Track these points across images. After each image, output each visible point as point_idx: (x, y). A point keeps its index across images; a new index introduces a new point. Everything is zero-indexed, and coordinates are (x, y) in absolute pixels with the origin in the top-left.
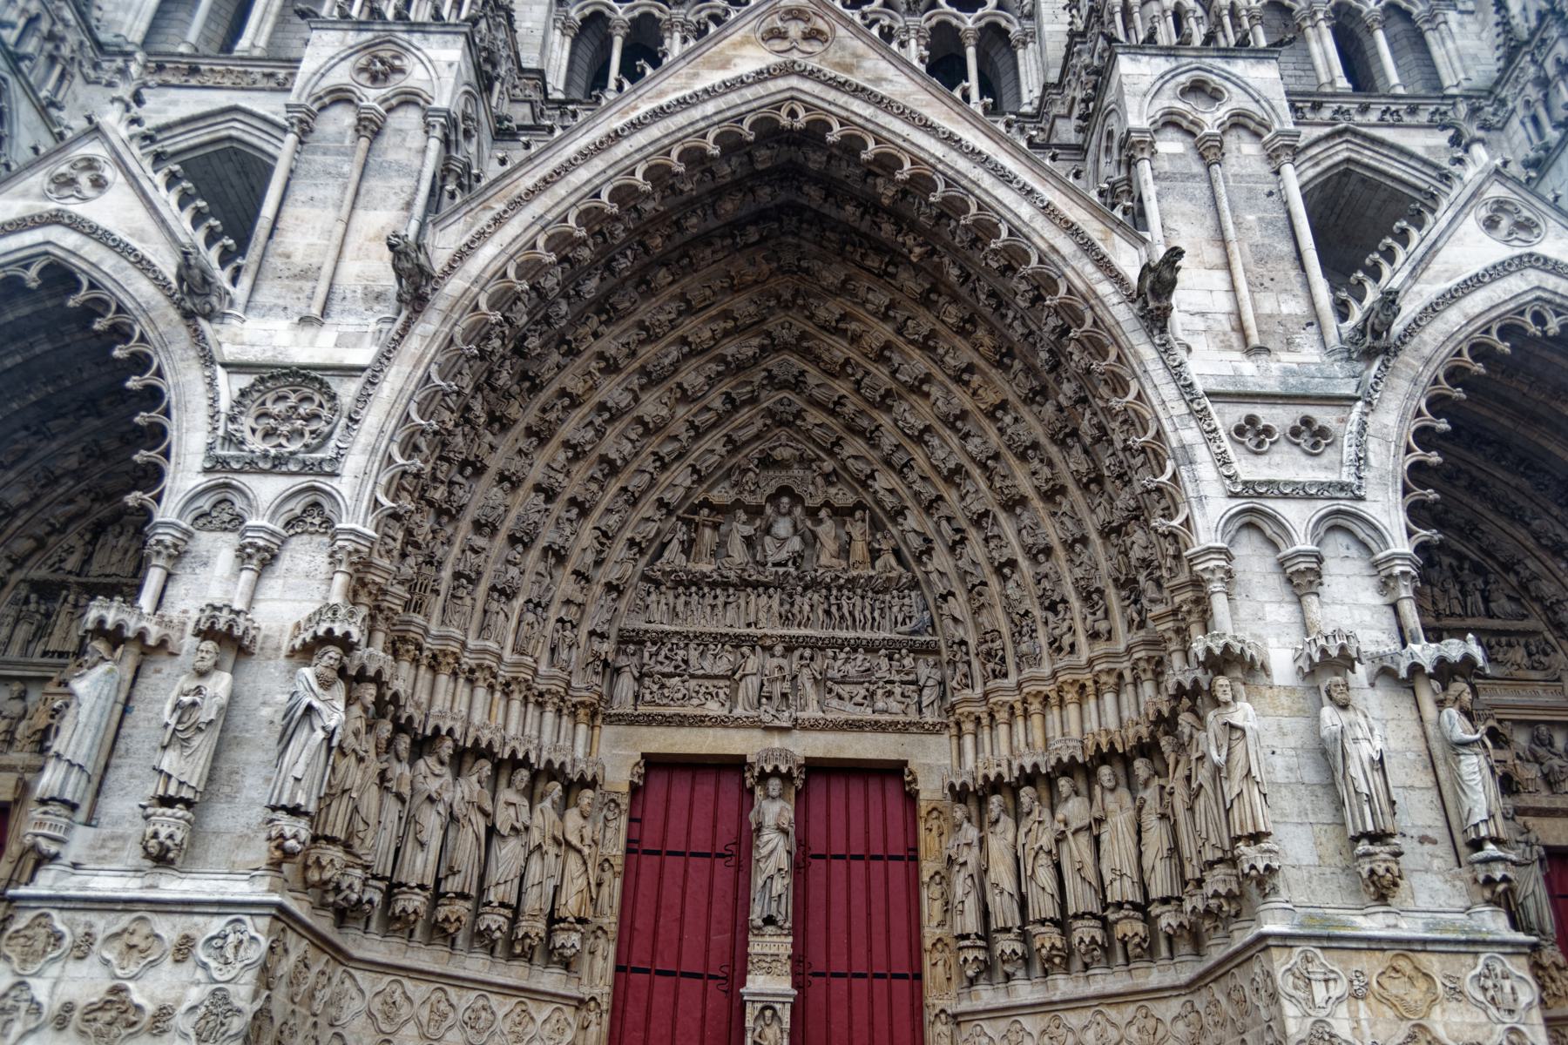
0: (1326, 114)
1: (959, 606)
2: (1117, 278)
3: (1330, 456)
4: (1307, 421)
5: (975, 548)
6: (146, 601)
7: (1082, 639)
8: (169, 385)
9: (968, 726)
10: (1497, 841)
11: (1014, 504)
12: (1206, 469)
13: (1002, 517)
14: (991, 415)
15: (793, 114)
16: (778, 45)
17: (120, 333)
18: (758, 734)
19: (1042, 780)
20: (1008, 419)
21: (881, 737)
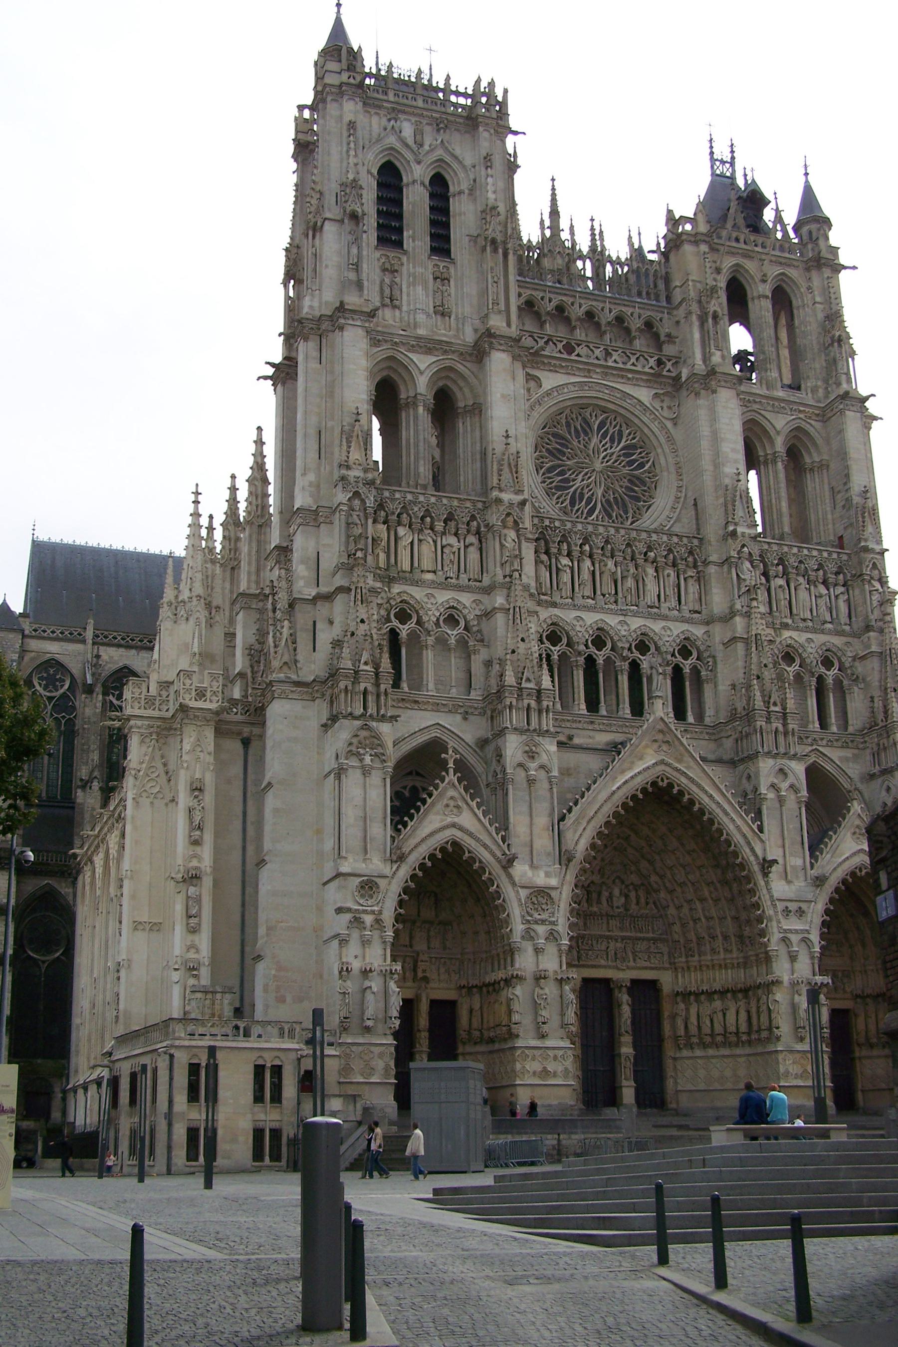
0: (810, 740)
1: (677, 928)
2: (756, 856)
3: (804, 919)
4: (800, 908)
5: (685, 910)
7: (722, 950)
9: (680, 970)
11: (702, 900)
12: (774, 924)
13: (697, 902)
14: (699, 868)
15: (662, 780)
16: (656, 745)
18: (616, 971)
19: (710, 995)
20: (704, 871)
21: (653, 972)
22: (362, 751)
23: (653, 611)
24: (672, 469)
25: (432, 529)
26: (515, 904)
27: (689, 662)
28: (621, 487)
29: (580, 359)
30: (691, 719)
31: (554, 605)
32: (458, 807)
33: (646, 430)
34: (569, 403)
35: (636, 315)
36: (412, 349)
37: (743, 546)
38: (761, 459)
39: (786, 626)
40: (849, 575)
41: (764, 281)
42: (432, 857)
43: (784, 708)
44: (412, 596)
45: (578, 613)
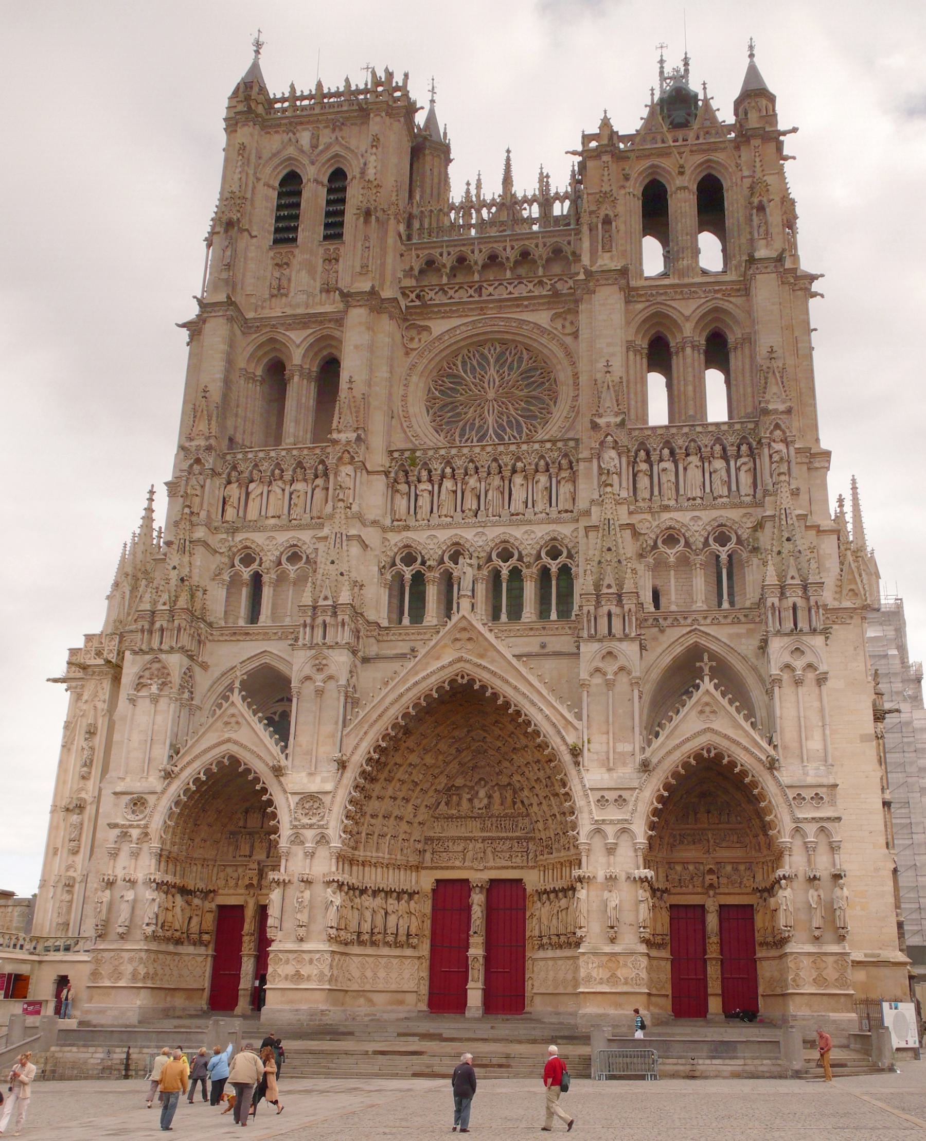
0: (689, 621)
6: (282, 869)
8: (274, 798)
10: (644, 928)
17: (257, 780)
22: (149, 682)
23: (516, 518)
24: (571, 382)
25: (281, 477)
26: (286, 810)
27: (558, 561)
28: (517, 409)
29: (471, 299)
30: (554, 616)
31: (407, 528)
32: (237, 723)
33: (545, 351)
34: (462, 344)
35: (541, 245)
36: (289, 327)
37: (606, 436)
38: (672, 350)
39: (666, 508)
40: (754, 444)
41: (681, 173)
42: (208, 771)
43: (620, 585)
44: (253, 542)
45: (433, 532)
